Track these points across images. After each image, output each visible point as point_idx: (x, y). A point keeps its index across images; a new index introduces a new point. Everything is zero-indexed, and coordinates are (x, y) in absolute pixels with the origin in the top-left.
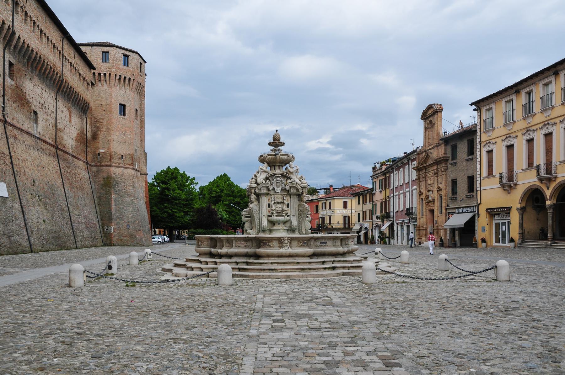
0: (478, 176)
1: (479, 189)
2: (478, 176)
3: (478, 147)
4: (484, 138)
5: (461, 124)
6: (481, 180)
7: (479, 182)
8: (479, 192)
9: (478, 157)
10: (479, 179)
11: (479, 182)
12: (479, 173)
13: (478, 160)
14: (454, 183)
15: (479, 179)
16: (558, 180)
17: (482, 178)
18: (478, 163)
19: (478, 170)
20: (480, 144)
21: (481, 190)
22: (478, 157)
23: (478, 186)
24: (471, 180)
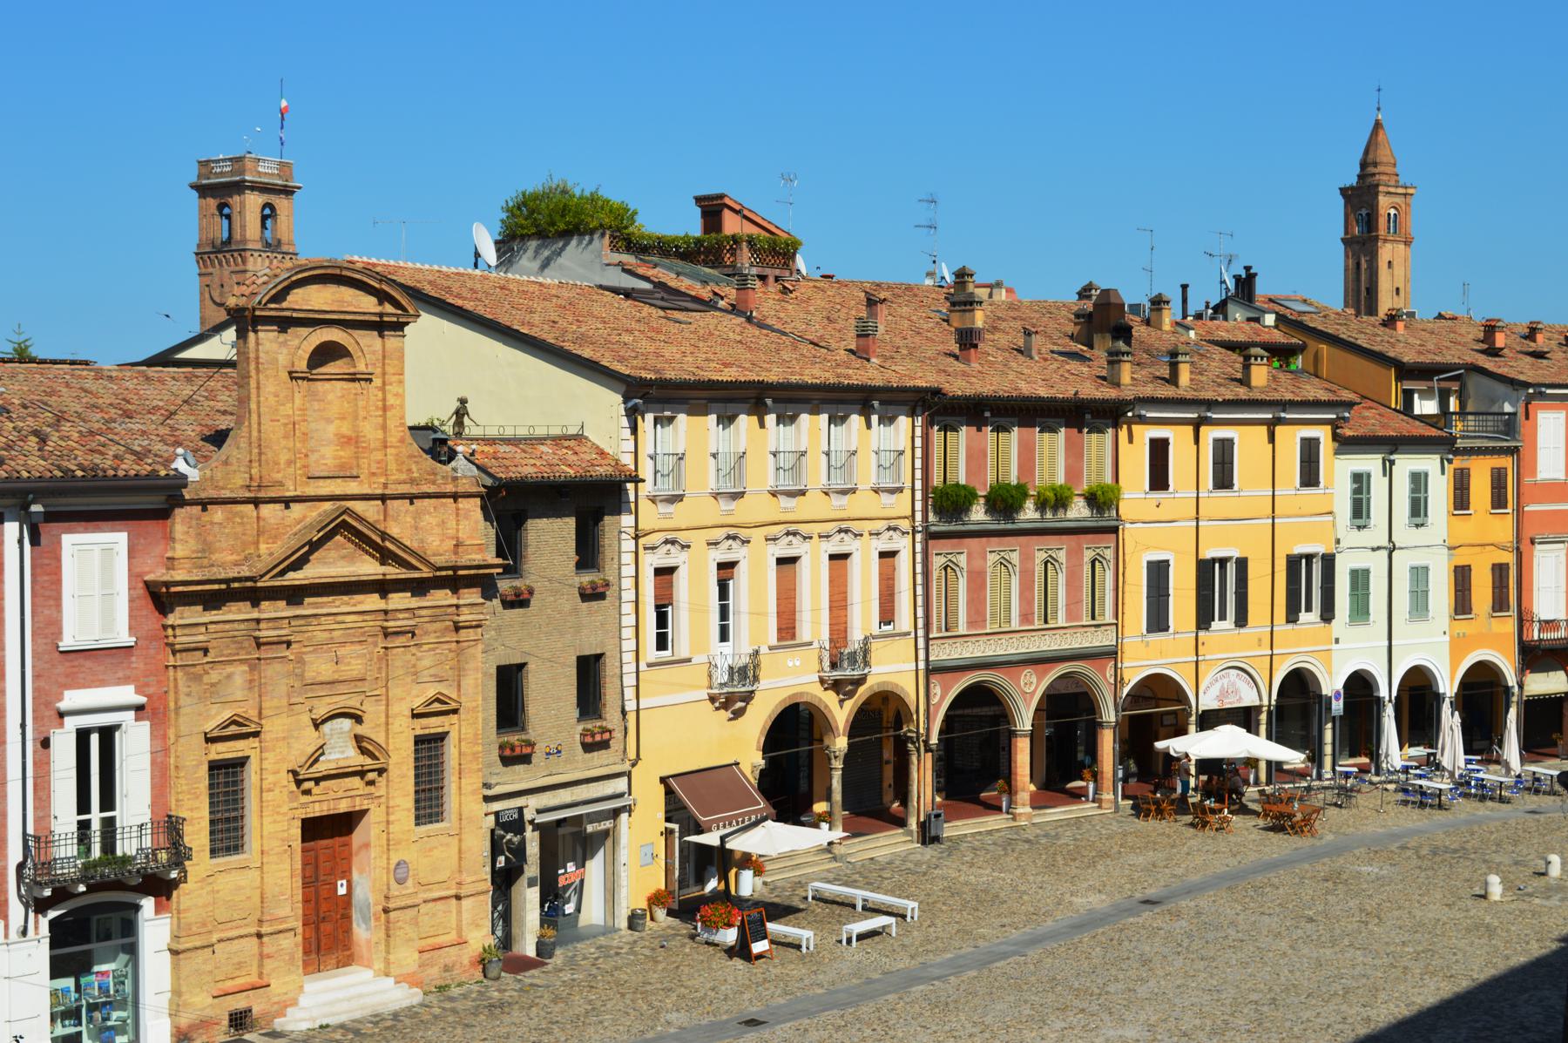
0: (629, 657)
1: (631, 706)
2: (629, 657)
3: (628, 545)
4: (650, 515)
5: (461, 413)
6: (638, 672)
7: (629, 680)
8: (632, 718)
9: (627, 583)
10: (629, 668)
11: (629, 680)
12: (629, 645)
13: (628, 595)
14: (510, 682)
15: (629, 668)
16: (870, 681)
17: (643, 667)
18: (628, 608)
19: (628, 633)
20: (636, 538)
21: (638, 711)
22: (627, 583)
23: (630, 693)
24: (589, 671)
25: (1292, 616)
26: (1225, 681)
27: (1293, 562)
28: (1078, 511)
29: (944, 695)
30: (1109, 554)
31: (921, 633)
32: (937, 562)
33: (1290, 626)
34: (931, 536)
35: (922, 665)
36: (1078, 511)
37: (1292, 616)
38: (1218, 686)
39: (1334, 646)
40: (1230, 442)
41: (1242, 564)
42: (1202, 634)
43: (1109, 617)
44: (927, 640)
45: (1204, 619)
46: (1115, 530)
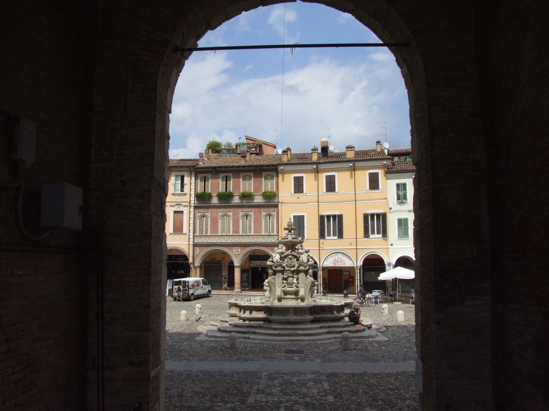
25: (366, 234)
26: (336, 257)
27: (366, 216)
28: (258, 200)
29: (201, 253)
30: (275, 214)
31: (191, 234)
32: (198, 215)
33: (366, 239)
34: (195, 207)
35: (191, 243)
36: (258, 200)
37: (366, 234)
38: (333, 258)
39: (390, 247)
40: (334, 176)
41: (340, 217)
42: (322, 241)
43: (275, 233)
44: (194, 236)
45: (322, 235)
46: (276, 206)
